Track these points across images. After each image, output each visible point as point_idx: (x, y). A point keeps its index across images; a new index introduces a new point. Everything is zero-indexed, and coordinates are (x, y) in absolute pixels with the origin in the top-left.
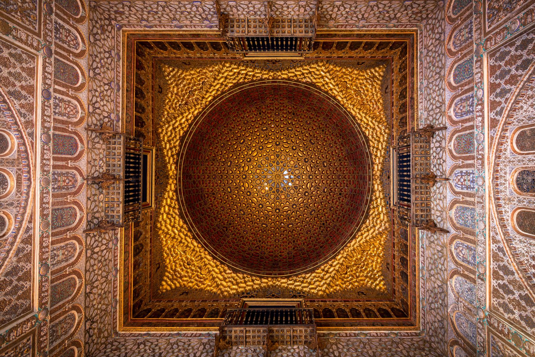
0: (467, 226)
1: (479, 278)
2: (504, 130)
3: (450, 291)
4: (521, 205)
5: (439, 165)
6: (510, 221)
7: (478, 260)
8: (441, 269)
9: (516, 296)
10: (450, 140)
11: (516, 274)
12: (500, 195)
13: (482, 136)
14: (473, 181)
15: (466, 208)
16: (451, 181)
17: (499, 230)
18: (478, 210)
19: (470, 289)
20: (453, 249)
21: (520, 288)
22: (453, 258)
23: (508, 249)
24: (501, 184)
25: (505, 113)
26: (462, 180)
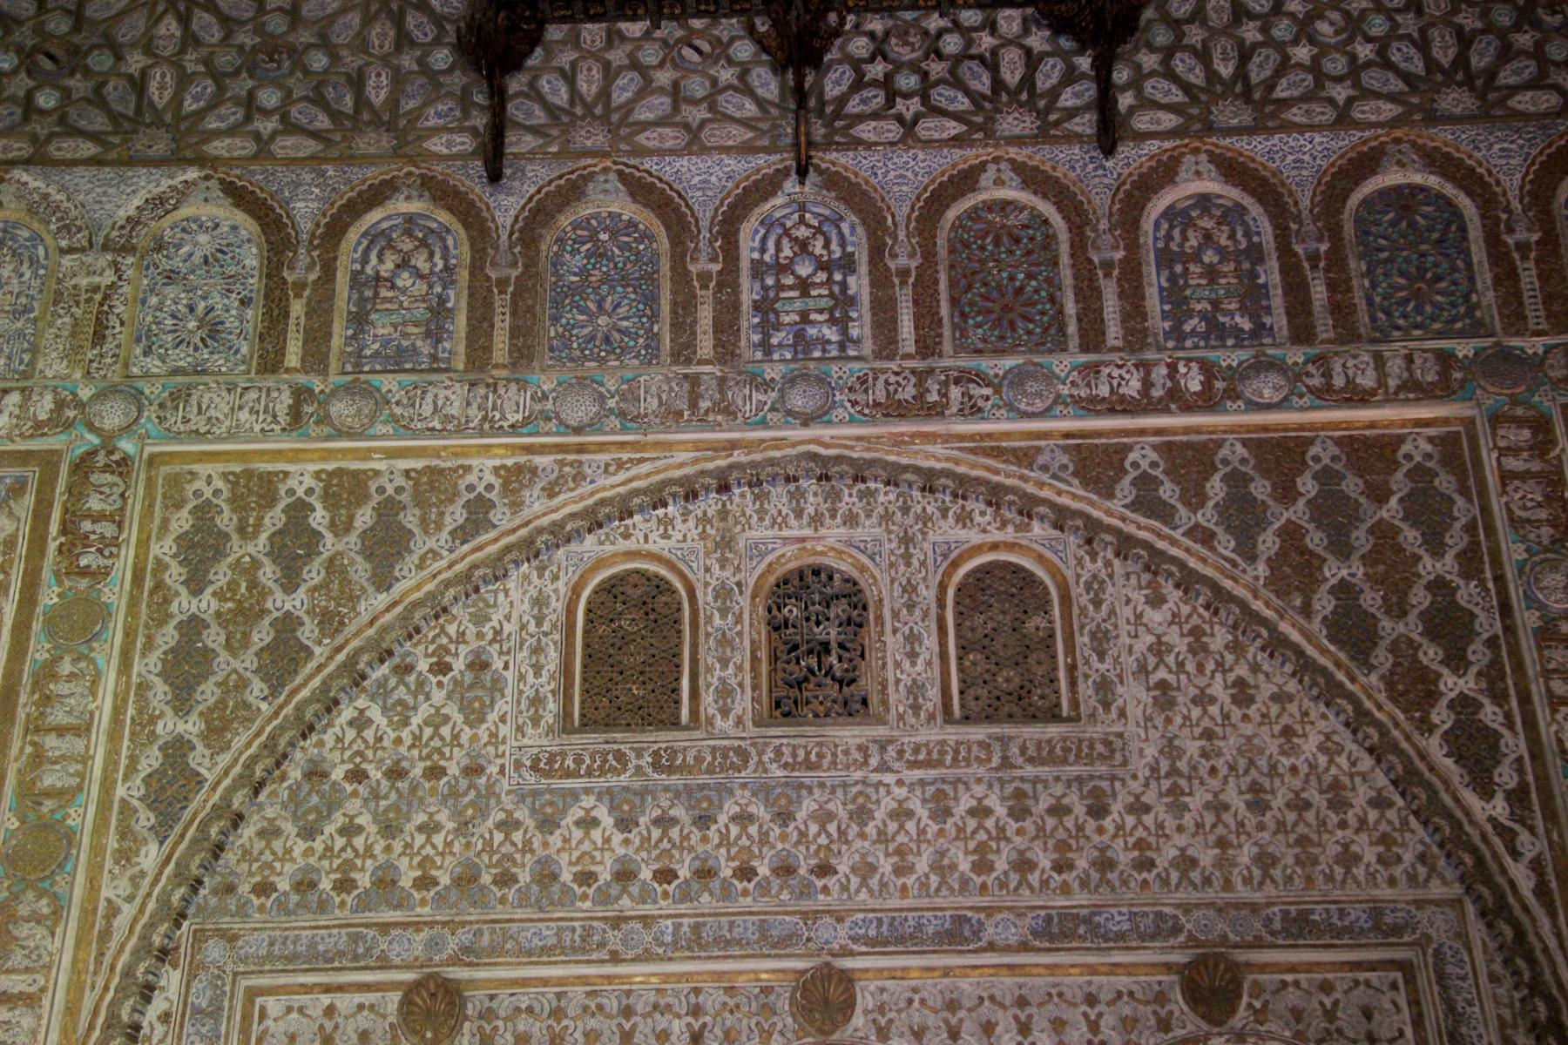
0: (557, 304)
1: (301, 395)
2: (1061, 518)
3: (147, 184)
4: (705, 597)
5: (887, 83)
6: (623, 545)
7: (388, 383)
8: (250, 105)
9: (280, 602)
10: (1032, 178)
11: (382, 599)
12: (741, 497)
13: (1039, 405)
14: (802, 344)
15: (651, 299)
16: (791, 185)
17: (570, 503)
18: (657, 384)
19: (213, 330)
20: (402, 205)
21: (330, 622)
22: (356, 208)
23: (492, 549)
24: (797, 496)
25: (1141, 527)
26: (804, 269)
